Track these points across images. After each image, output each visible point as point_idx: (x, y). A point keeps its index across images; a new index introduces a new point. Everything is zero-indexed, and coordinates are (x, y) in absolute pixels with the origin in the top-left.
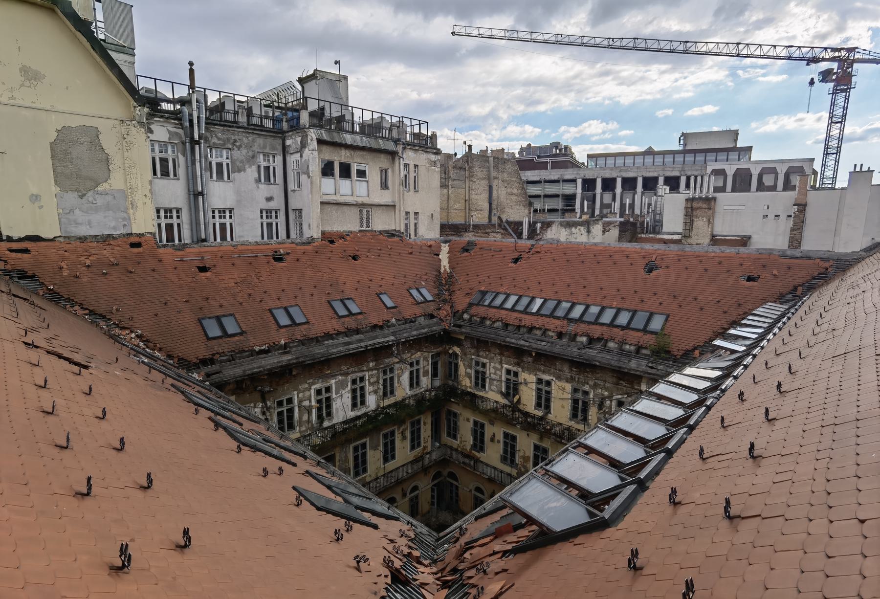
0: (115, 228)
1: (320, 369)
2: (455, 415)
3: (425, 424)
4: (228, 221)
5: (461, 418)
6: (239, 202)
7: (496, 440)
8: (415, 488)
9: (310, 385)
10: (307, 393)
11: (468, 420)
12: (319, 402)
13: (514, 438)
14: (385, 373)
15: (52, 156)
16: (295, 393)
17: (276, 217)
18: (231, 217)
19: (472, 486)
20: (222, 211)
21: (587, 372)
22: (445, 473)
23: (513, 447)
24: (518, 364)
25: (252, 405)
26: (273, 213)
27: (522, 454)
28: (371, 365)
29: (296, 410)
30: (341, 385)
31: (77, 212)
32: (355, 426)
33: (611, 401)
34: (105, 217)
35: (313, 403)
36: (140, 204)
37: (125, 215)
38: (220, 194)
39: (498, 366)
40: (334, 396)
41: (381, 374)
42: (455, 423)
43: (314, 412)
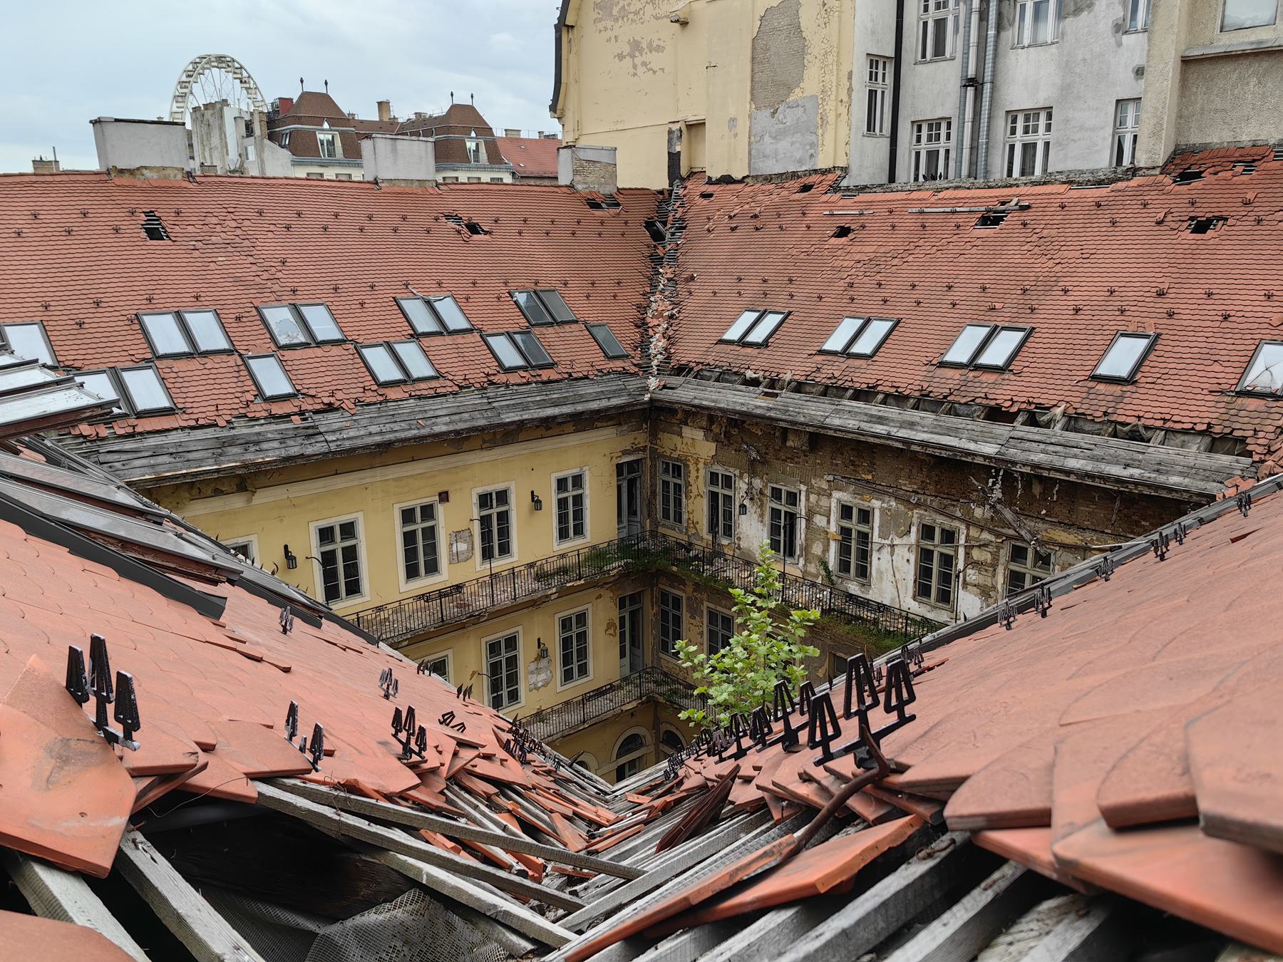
0: (800, 161)
1: (853, 463)
4: (1040, 138)
6: (1065, 90)
9: (834, 486)
10: (824, 502)
12: (845, 532)
14: (1018, 554)
15: (753, 59)
16: (803, 488)
17: (1048, 128)
18: (1048, 128)
20: (934, 125)
25: (737, 472)
26: (1043, 116)
28: (978, 512)
29: (801, 525)
30: (895, 525)
31: (767, 138)
32: (876, 622)
34: (792, 144)
35: (833, 528)
36: (831, 117)
37: (813, 138)
38: (1027, 76)
40: (876, 538)
41: (1005, 553)
43: (833, 547)
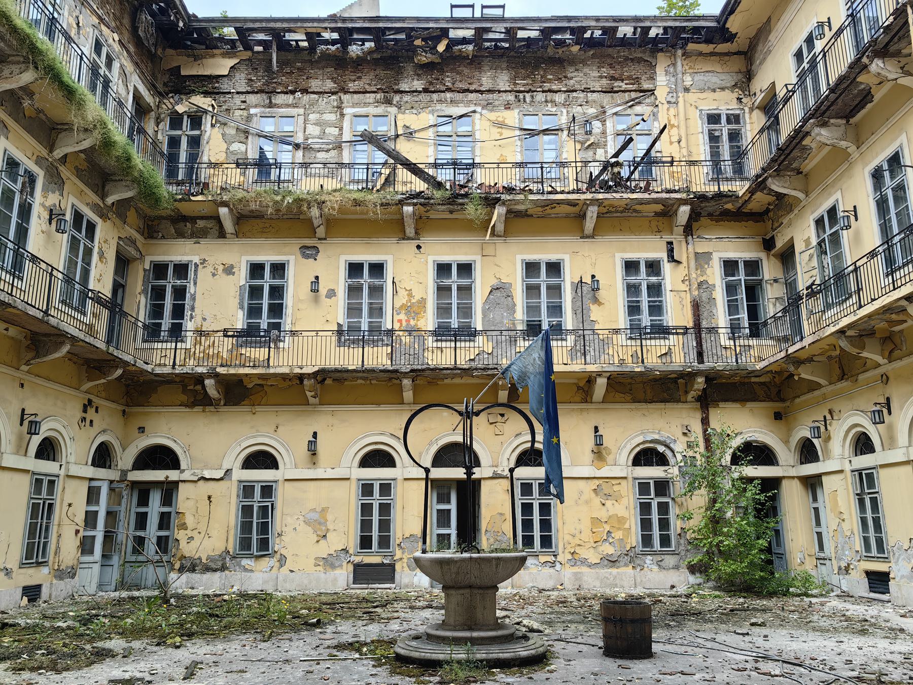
2: (182, 270)
3: (102, 255)
5: (204, 274)
7: (323, 290)
8: (48, 449)
11: (229, 270)
13: (377, 269)
19: (233, 459)
21: (550, 81)
22: (125, 458)
23: (377, 291)
24: (388, 102)
27: (402, 299)
33: (603, 122)
39: (332, 117)
42: (180, 293)
